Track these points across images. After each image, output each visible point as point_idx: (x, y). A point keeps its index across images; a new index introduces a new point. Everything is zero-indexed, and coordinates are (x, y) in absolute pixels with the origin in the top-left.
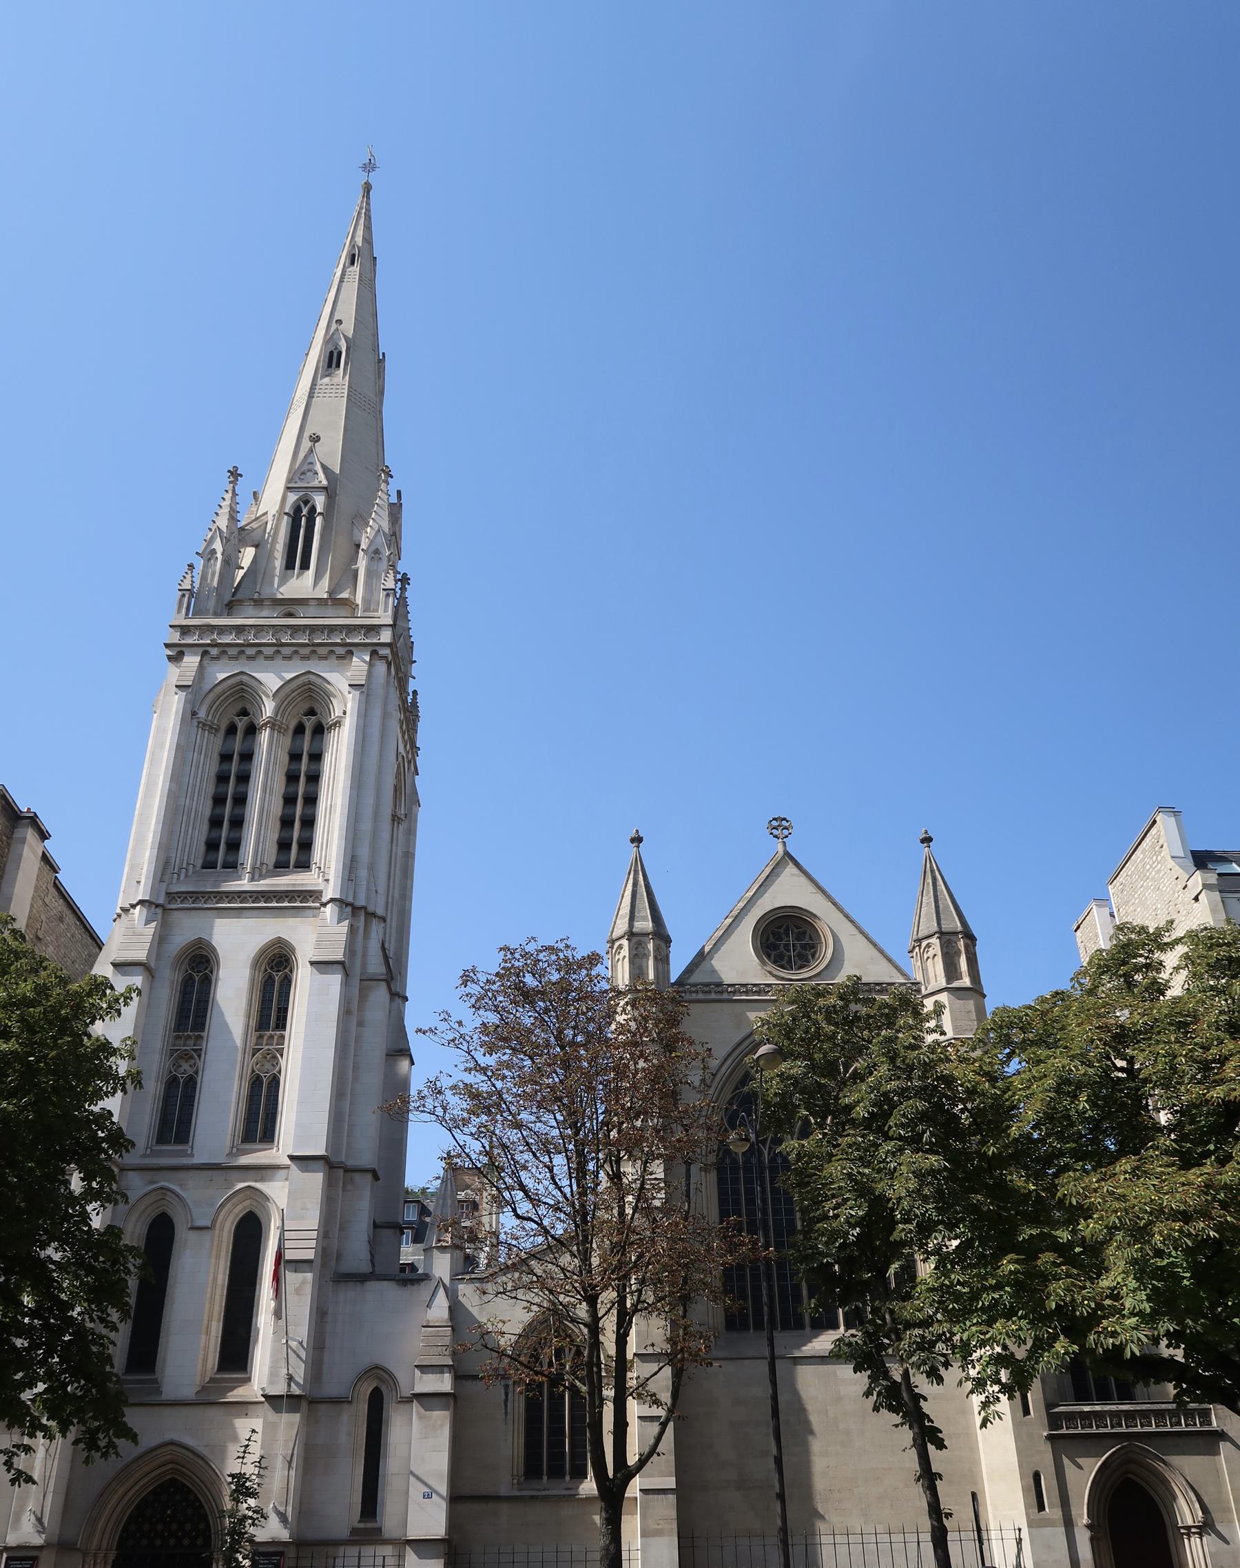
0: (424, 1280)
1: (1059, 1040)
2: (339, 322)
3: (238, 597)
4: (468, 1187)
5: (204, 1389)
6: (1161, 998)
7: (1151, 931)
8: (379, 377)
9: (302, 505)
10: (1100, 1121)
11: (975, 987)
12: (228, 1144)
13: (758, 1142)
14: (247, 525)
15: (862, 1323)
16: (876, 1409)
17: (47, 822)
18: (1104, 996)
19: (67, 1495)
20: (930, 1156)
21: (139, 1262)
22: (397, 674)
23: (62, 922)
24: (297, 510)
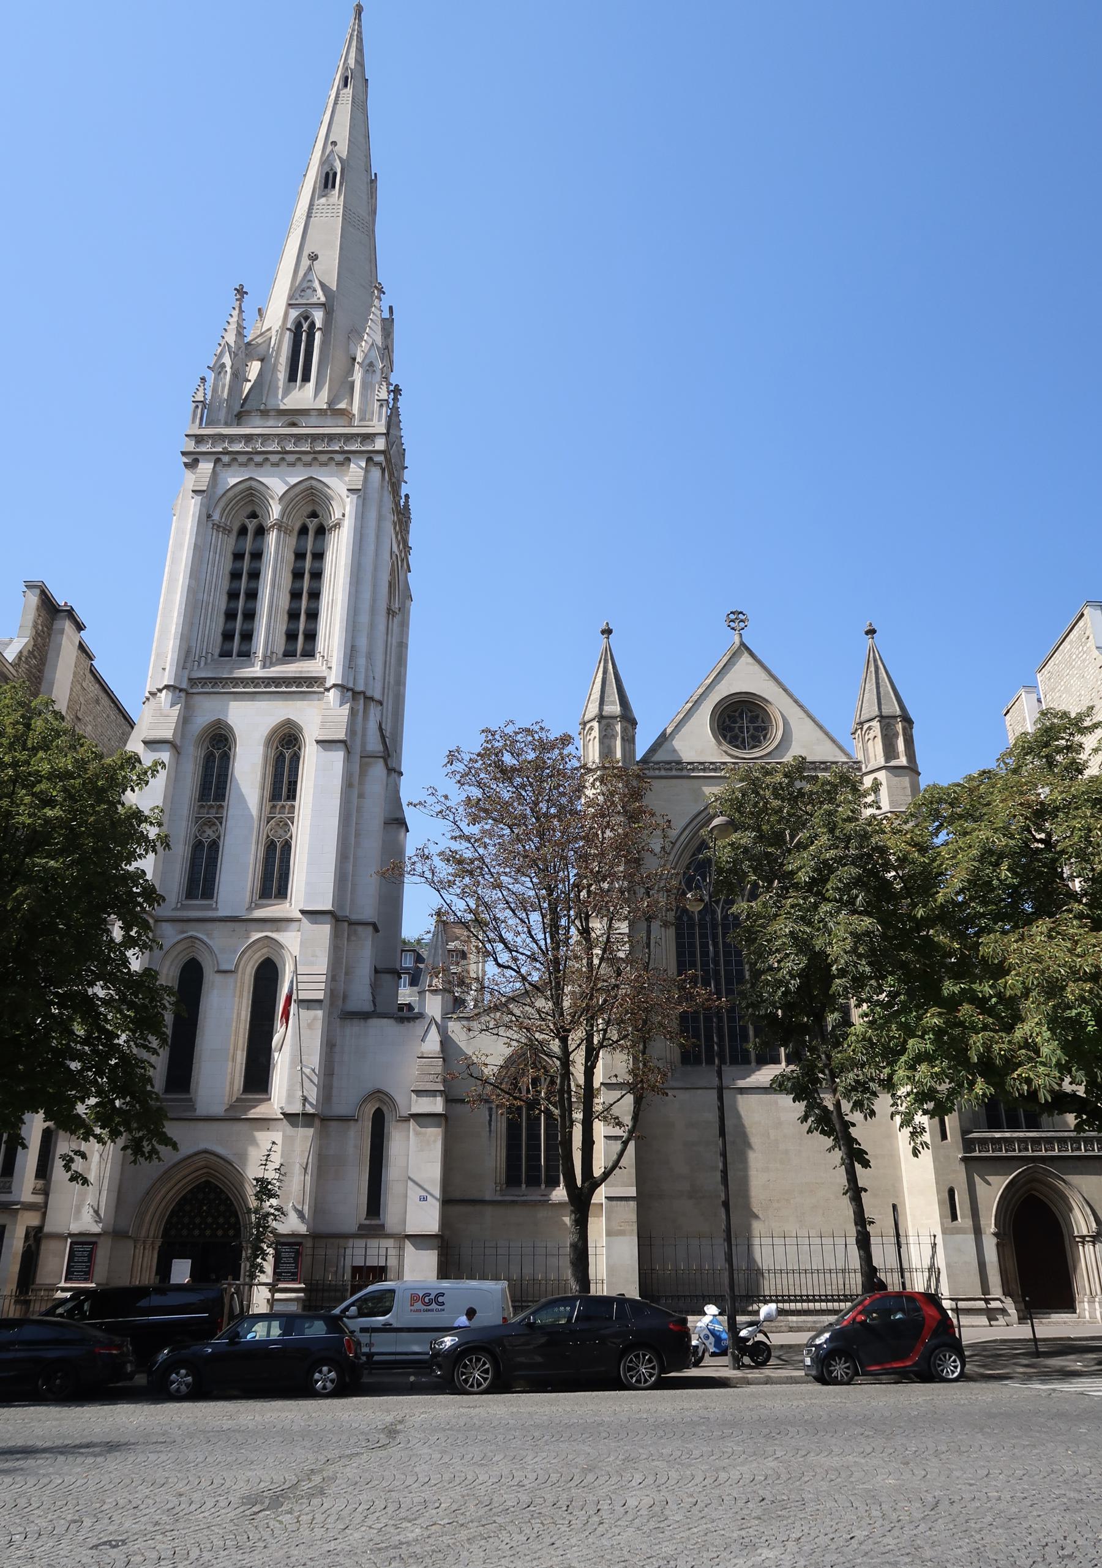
0: (417, 1018)
1: (985, 814)
2: (334, 143)
3: (246, 408)
4: (457, 938)
5: (232, 1107)
6: (1080, 777)
7: (1073, 715)
8: (372, 198)
9: (303, 321)
10: (1018, 886)
11: (912, 766)
12: (248, 899)
13: (711, 901)
14: (252, 340)
15: (800, 1060)
16: (810, 1131)
17: (82, 615)
18: (1026, 774)
19: (119, 1192)
20: (865, 918)
21: (173, 999)
22: (390, 479)
23: (98, 704)
24: (299, 326)
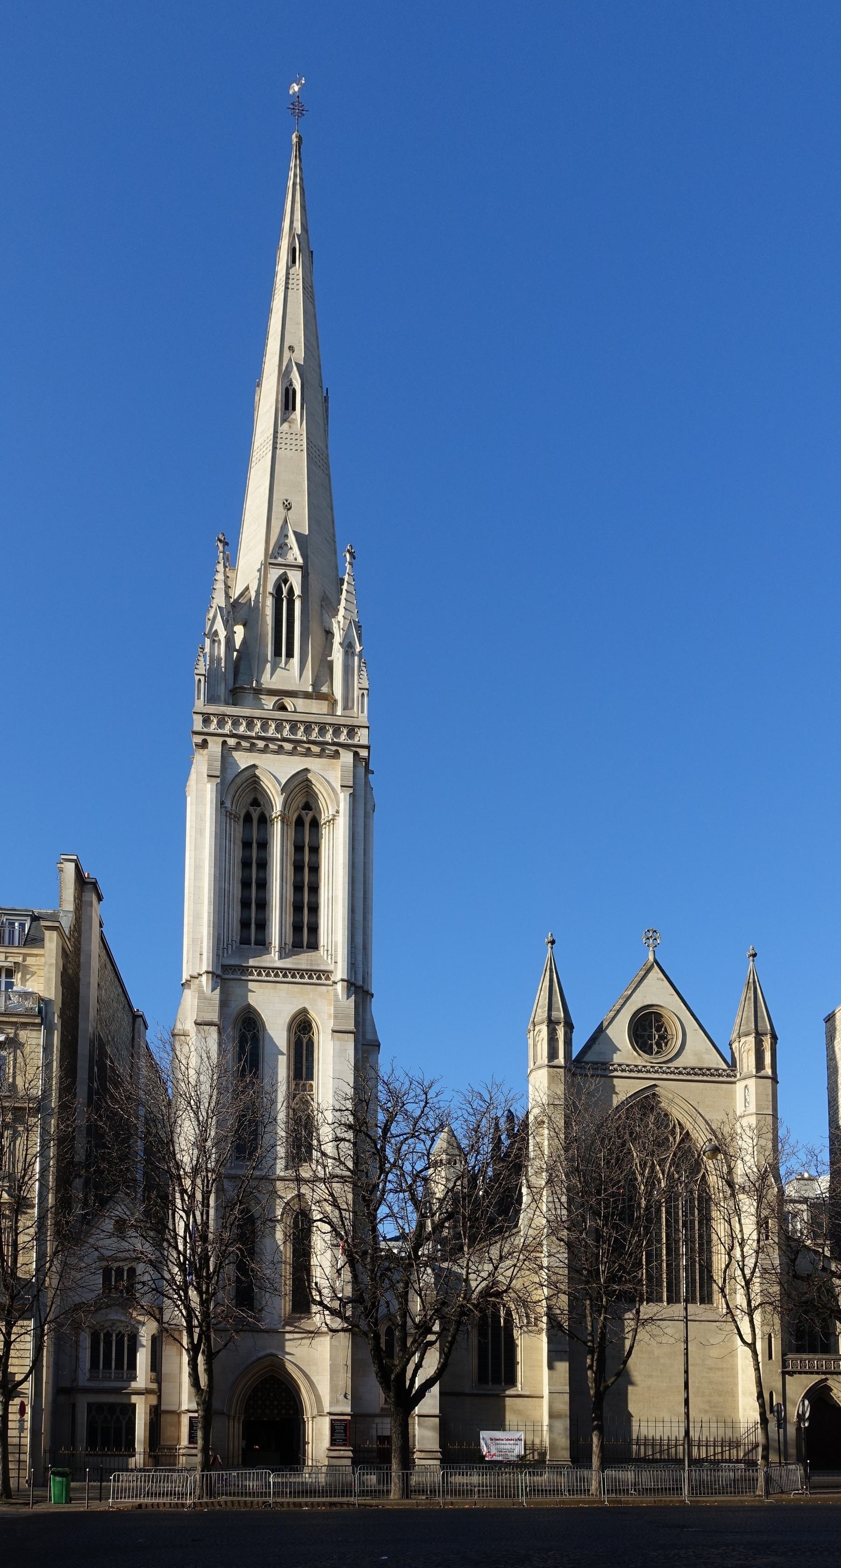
2: (291, 348)
